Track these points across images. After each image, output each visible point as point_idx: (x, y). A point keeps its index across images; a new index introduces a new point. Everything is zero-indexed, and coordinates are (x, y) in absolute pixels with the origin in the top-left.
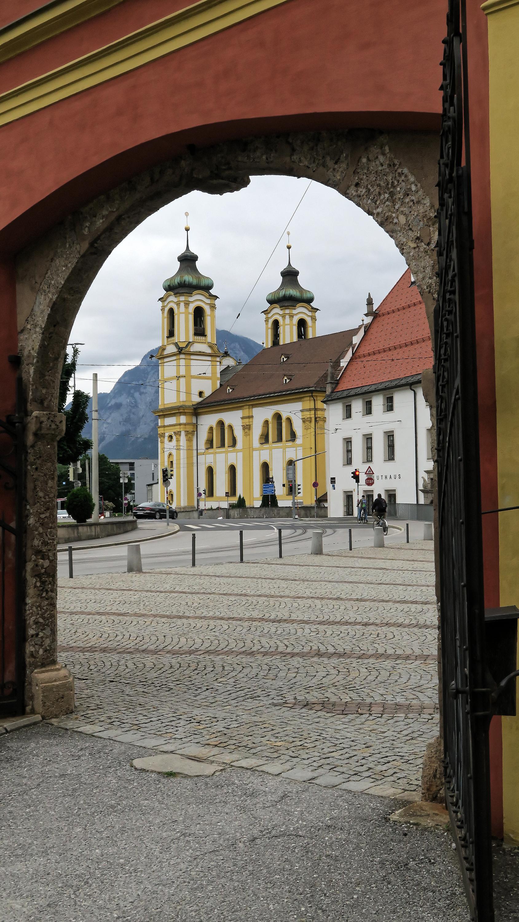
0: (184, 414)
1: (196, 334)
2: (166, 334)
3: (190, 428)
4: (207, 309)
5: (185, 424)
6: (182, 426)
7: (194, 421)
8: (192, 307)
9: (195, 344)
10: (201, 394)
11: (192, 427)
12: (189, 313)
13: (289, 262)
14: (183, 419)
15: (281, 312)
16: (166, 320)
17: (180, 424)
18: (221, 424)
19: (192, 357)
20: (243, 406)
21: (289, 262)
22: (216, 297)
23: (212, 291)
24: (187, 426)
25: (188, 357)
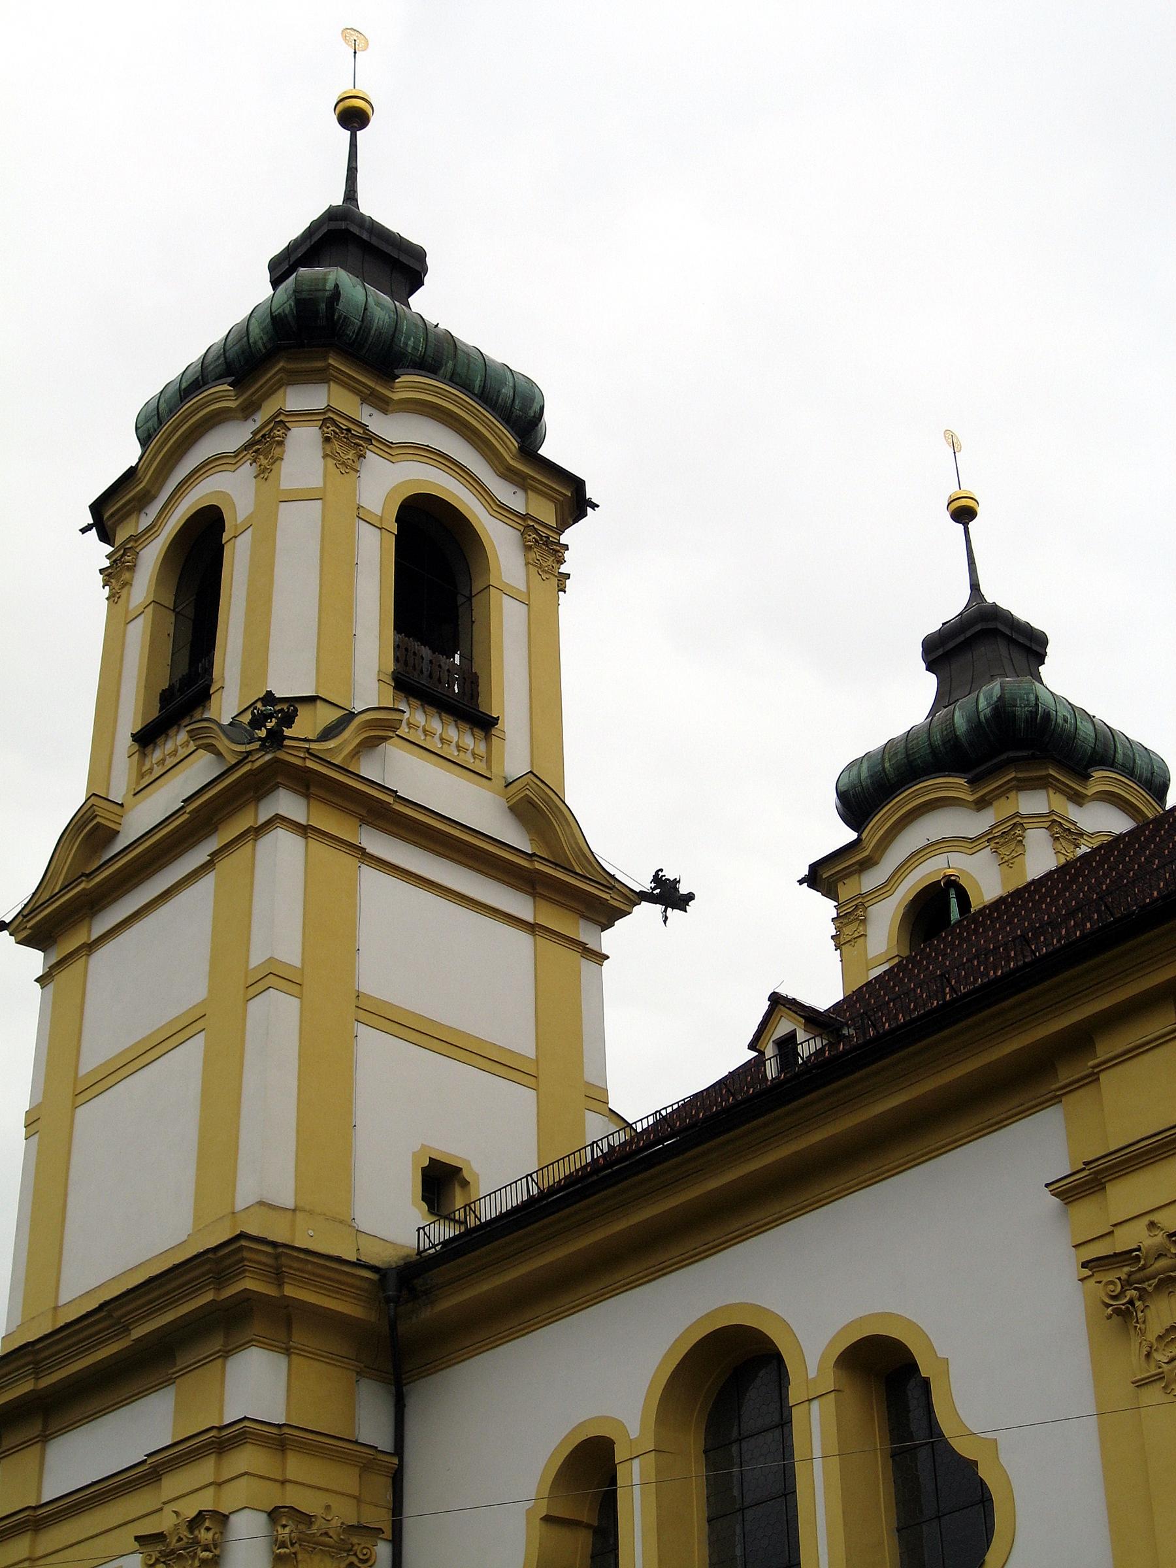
0: (281, 1324)
1: (408, 682)
2: (131, 717)
3: (328, 1494)
5: (280, 1439)
6: (246, 1459)
7: (374, 1430)
8: (383, 483)
10: (439, 1181)
11: (345, 1478)
12: (361, 514)
13: (975, 587)
14: (256, 1384)
15: (977, 824)
16: (138, 633)
17: (223, 1441)
18: (732, 1377)
20: (1080, 1040)
21: (975, 587)
24: (296, 1466)
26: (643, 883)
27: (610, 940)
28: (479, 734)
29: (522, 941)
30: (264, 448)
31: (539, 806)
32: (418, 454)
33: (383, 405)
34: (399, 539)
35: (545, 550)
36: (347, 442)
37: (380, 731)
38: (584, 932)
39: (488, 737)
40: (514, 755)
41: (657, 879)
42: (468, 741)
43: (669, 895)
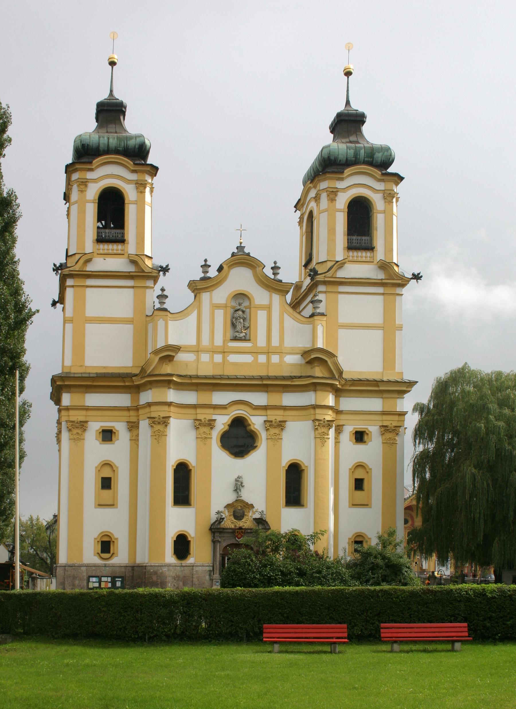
1: (351, 247)
4: (377, 201)
8: (342, 201)
9: (348, 266)
19: (341, 289)
22: (398, 178)
23: (390, 170)
25: (330, 288)
26: (411, 277)
27: (404, 291)
28: (371, 251)
29: (381, 298)
30: (317, 198)
31: (385, 266)
32: (354, 184)
33: (342, 179)
34: (348, 213)
35: (389, 197)
36: (333, 194)
37: (340, 265)
38: (398, 290)
39: (373, 251)
40: (380, 254)
41: (413, 275)
42: (369, 254)
43: (417, 277)
